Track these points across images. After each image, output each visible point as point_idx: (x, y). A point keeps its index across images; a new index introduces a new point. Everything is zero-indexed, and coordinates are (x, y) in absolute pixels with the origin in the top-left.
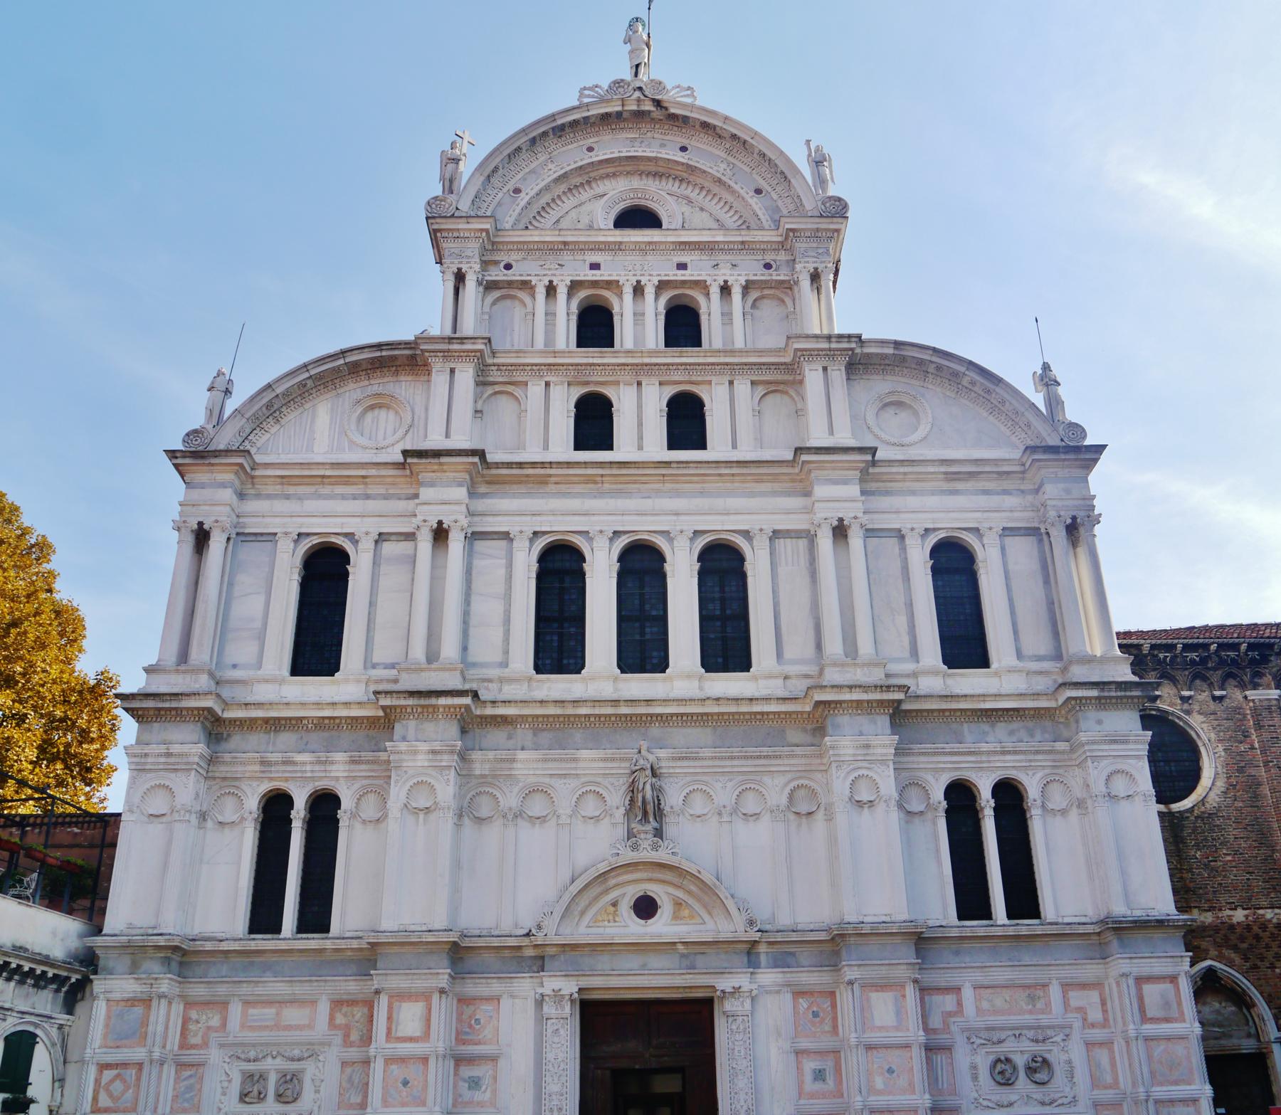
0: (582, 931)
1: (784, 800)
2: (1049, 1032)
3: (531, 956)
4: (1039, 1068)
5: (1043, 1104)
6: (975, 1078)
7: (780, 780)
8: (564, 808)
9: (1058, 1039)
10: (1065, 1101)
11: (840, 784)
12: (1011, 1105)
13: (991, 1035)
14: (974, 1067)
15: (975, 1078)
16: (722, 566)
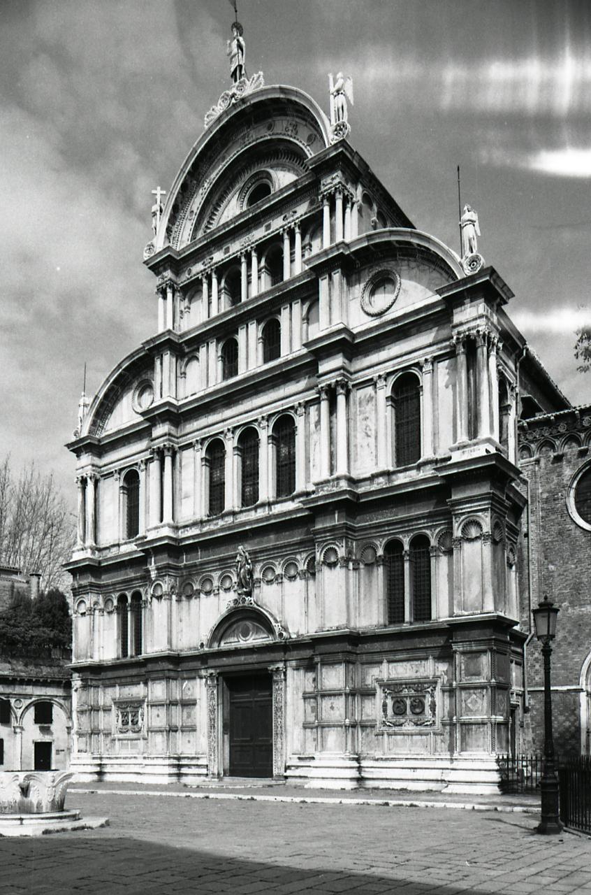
0: (224, 646)
1: (305, 567)
2: (426, 686)
3: (203, 658)
4: (418, 706)
5: (417, 725)
6: (385, 711)
7: (304, 555)
8: (216, 583)
9: (429, 690)
10: (428, 723)
11: (319, 557)
12: (401, 725)
13: (393, 687)
14: (385, 705)
15: (385, 711)
16: (284, 428)
